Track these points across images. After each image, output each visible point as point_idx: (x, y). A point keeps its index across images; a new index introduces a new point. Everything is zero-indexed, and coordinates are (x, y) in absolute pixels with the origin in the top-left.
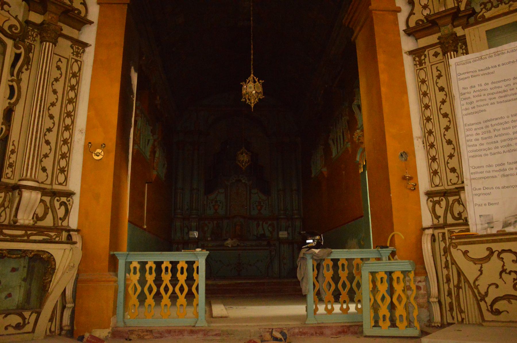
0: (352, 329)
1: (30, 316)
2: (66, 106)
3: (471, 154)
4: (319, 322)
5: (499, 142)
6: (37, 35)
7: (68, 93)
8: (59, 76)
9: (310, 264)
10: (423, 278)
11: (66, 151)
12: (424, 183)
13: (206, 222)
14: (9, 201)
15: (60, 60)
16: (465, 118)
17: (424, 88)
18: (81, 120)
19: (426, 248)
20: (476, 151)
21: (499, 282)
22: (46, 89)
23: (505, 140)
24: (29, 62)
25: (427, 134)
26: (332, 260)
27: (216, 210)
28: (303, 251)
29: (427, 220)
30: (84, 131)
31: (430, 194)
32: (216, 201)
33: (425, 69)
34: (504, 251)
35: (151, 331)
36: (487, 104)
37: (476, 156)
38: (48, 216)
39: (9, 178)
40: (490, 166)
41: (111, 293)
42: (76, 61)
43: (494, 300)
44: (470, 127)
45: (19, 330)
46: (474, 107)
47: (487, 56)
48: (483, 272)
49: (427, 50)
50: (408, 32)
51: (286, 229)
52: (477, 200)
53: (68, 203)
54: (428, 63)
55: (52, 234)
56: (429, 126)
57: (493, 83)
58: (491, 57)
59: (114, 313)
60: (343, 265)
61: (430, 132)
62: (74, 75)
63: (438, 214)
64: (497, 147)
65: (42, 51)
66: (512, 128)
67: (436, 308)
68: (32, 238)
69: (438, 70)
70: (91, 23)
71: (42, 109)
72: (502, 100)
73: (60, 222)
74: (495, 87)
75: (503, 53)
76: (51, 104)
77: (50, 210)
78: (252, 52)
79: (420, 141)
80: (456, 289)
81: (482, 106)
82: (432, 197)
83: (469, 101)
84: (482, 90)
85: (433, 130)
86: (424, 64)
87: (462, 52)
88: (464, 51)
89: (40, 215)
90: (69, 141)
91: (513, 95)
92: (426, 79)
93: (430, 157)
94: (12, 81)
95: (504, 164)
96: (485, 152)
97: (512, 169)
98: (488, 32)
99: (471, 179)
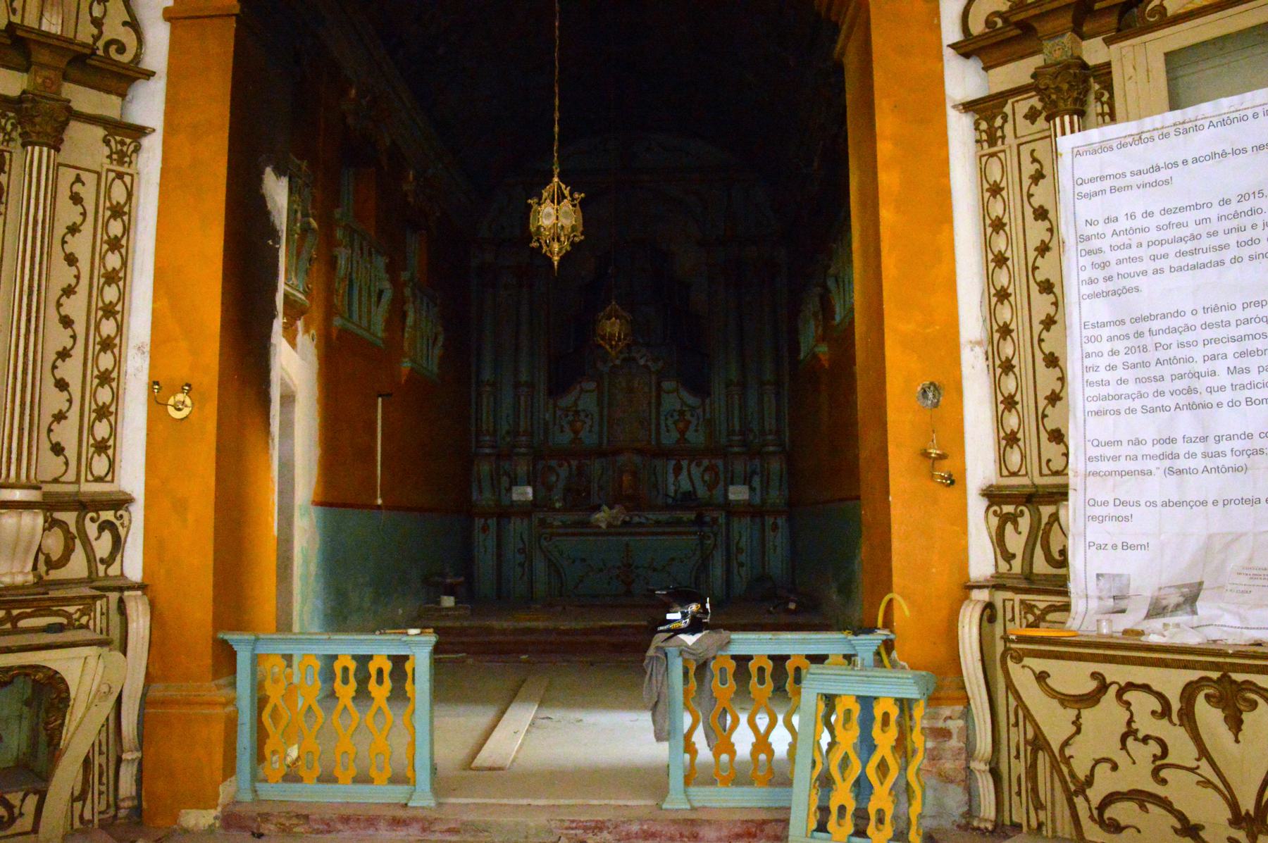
0: (768, 829)
1: (23, 800)
2: (101, 291)
3: (1093, 406)
4: (696, 804)
5: (1168, 378)
7: (103, 258)
8: (79, 220)
10: (961, 708)
11: (108, 401)
12: (980, 464)
13: (553, 463)
15: (78, 179)
17: (997, 209)
18: (139, 325)
19: (967, 641)
20: (1105, 398)
21: (1120, 757)
22: (41, 263)
23: (1181, 376)
25: (996, 336)
26: (734, 657)
27: (576, 432)
28: (658, 639)
29: (982, 562)
30: (147, 349)
31: (993, 496)
32: (577, 413)
33: (1002, 155)
34: (1131, 686)
35: (307, 817)
36: (1144, 273)
37: (1105, 413)
38: (73, 557)
40: (1138, 442)
41: (218, 731)
42: (120, 176)
43: (1106, 797)
44: (1096, 332)
46: (1110, 278)
47: (1156, 134)
48: (1083, 727)
49: (1010, 101)
50: (962, 51)
51: (747, 480)
52: (1096, 532)
53: (118, 523)
55: (71, 609)
56: (1004, 314)
57: (1166, 211)
58: (1166, 136)
59: (230, 769)
60: (761, 670)
61: (1005, 331)
62: (117, 212)
63: (1011, 550)
64: (1162, 394)
66: (1201, 344)
67: (985, 786)
68: (23, 623)
69: (1035, 160)
70: (149, 75)
71: (34, 314)
73: (101, 568)
74: (1170, 225)
75: (1197, 128)
76: (63, 290)
77: (77, 541)
79: (979, 351)
80: (1029, 748)
81: (1129, 275)
82: (999, 504)
83: (1097, 259)
84: (1135, 231)
85: (1013, 326)
86: (1000, 142)
87: (1099, 111)
88: (1106, 109)
89: (55, 557)
90: (114, 375)
91: (1215, 249)
92: (1003, 184)
93: (1000, 398)
95: (1172, 441)
96: (1129, 403)
97: (1194, 455)
98: (1172, 59)
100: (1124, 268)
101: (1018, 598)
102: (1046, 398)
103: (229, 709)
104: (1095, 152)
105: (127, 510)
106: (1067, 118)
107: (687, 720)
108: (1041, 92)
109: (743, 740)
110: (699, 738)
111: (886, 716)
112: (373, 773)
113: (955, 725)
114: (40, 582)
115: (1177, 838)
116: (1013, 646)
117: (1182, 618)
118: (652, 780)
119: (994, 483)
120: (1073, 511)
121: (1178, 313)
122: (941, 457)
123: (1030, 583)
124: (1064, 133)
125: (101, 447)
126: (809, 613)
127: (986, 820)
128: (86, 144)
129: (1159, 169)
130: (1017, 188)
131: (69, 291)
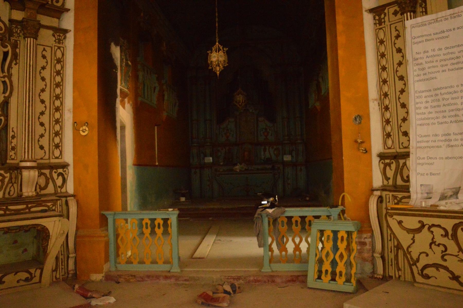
0: (300, 278)
1: (35, 271)
2: (54, 90)
3: (419, 122)
4: (274, 270)
6: (21, 32)
7: (54, 78)
8: (45, 64)
9: (266, 221)
10: (369, 234)
11: (59, 130)
12: (377, 145)
14: (16, 178)
15: (44, 50)
16: (416, 84)
17: (382, 49)
19: (372, 210)
20: (424, 119)
23: (452, 110)
24: (17, 57)
25: (382, 97)
26: (287, 217)
28: (259, 211)
29: (378, 181)
30: (72, 110)
31: (382, 156)
33: (384, 29)
34: (433, 225)
35: (134, 276)
36: (439, 72)
39: (13, 159)
40: (436, 135)
41: (102, 245)
42: (59, 48)
44: (420, 94)
45: (29, 282)
46: (425, 74)
47: (443, 19)
49: (387, 8)
51: (290, 153)
52: (420, 169)
53: (64, 173)
54: (387, 23)
55: (49, 204)
56: (386, 89)
57: (447, 48)
58: (447, 19)
59: (107, 259)
60: (297, 222)
61: (386, 95)
62: (59, 61)
63: (388, 176)
64: (445, 117)
65: (26, 45)
67: (379, 263)
68: (33, 209)
69: (397, 30)
70: (68, 10)
72: (453, 67)
73: (59, 189)
76: (41, 90)
77: (50, 180)
78: (217, 19)
79: (376, 103)
80: (395, 249)
81: (433, 73)
82: (384, 160)
83: (420, 67)
84: (435, 56)
85: (389, 93)
86: (383, 24)
87: (421, 10)
88: (424, 10)
89: (43, 185)
92: (385, 40)
93: (384, 120)
94: (4, 77)
95: (449, 135)
96: (432, 121)
97: (457, 140)
99: (417, 148)
100: (430, 70)
101: (391, 194)
102: (402, 120)
103: (106, 238)
104: (420, 26)
105: (67, 168)
106: (409, 14)
107: (270, 240)
108: (399, 4)
109: (290, 247)
110: (274, 246)
111: (342, 238)
112: (158, 260)
113: (368, 241)
114: (38, 195)
115: (451, 281)
116: (390, 211)
117: (453, 200)
118: (257, 262)
119: (382, 151)
120: (411, 162)
121: (451, 87)
122: (362, 142)
123: (396, 188)
124: (407, 20)
125: (57, 146)
126: (315, 202)
127: (379, 275)
128: (46, 36)
129: (444, 32)
130: (390, 41)
131: (43, 90)
